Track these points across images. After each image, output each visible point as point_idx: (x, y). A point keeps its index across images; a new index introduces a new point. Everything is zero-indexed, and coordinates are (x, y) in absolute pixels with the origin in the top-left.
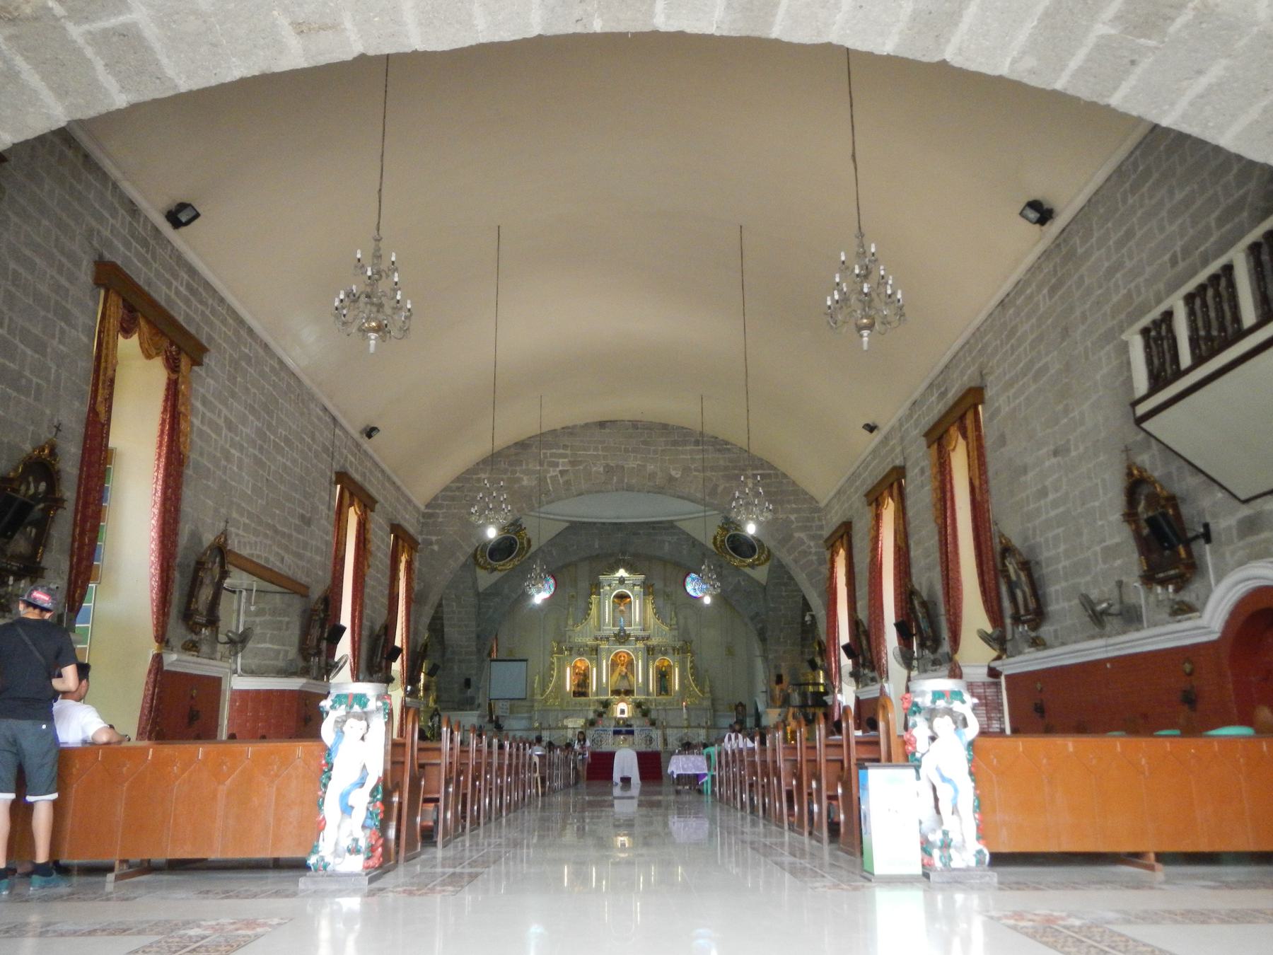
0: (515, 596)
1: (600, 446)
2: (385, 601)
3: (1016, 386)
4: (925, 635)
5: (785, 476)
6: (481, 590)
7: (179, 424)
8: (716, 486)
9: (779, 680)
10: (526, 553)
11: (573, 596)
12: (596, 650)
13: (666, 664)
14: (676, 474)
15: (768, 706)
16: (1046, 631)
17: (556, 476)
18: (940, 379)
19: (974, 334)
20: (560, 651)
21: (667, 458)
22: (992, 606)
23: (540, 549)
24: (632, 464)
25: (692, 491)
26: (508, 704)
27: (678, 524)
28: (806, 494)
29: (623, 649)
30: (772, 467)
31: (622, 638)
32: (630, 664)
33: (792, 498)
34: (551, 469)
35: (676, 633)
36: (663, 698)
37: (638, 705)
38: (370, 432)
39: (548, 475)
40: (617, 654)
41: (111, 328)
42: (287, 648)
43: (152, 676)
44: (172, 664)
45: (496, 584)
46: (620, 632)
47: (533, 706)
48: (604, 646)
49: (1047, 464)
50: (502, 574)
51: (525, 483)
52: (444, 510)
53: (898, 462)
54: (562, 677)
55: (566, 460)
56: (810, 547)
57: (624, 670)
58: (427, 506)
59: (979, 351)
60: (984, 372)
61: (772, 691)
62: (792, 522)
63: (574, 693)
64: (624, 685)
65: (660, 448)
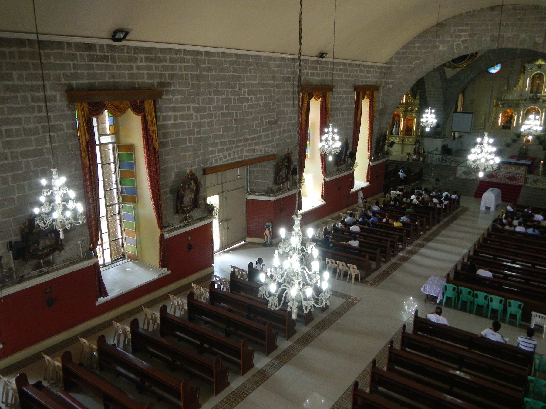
1: (489, 23)
2: (352, 126)
6: (448, 78)
10: (475, 58)
17: (460, 44)
21: (535, 29)
34: (457, 40)
39: (455, 43)
42: (268, 182)
46: (533, 97)
50: (461, 69)
51: (441, 48)
52: (396, 65)
54: (497, 119)
55: (467, 33)
58: (387, 63)
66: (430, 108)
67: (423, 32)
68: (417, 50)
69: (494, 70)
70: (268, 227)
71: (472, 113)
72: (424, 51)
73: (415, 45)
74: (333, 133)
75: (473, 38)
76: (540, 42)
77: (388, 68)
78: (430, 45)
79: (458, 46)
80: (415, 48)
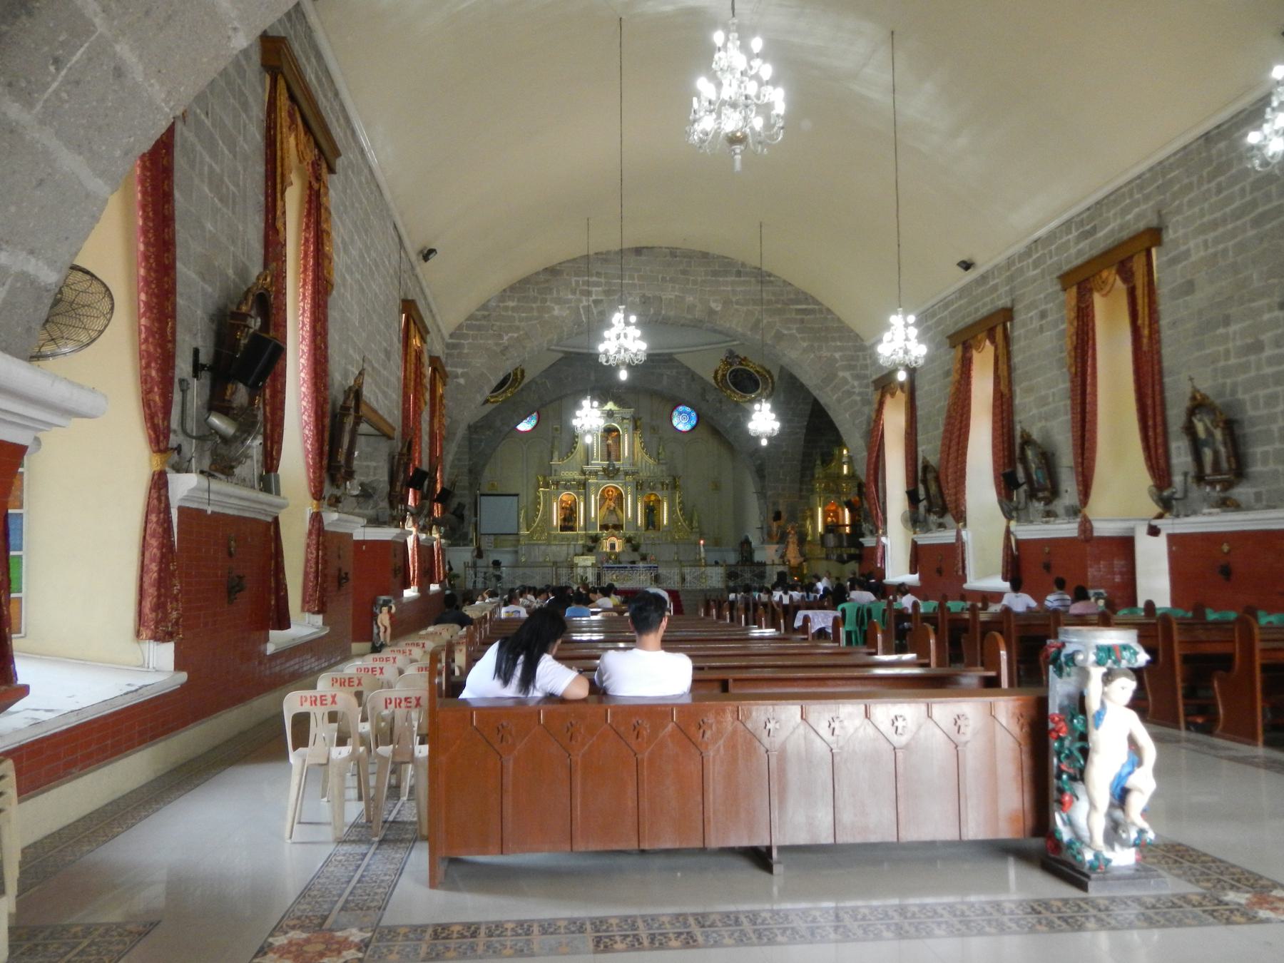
0: (507, 429)
1: (636, 275)
3: (1221, 230)
4: (1036, 486)
5: (829, 311)
7: (323, 244)
8: (758, 321)
9: (777, 516)
11: (556, 429)
12: (583, 485)
13: (653, 498)
14: (717, 307)
15: (763, 543)
16: (1241, 492)
18: (1085, 215)
19: (1151, 169)
20: (547, 485)
22: (1158, 463)
23: (533, 381)
24: (669, 294)
25: (733, 326)
26: (492, 538)
27: (676, 356)
28: (852, 331)
29: (611, 484)
30: (816, 302)
31: (610, 473)
32: (620, 498)
33: (836, 335)
35: (664, 468)
36: (652, 534)
37: (629, 540)
38: (427, 254)
39: (581, 305)
40: (603, 491)
41: (284, 124)
43: (314, 537)
44: (333, 523)
45: (486, 416)
47: (519, 541)
48: (592, 480)
49: (1266, 317)
50: (495, 405)
51: (556, 312)
53: (1004, 302)
54: (548, 512)
56: (853, 387)
57: (613, 505)
58: (451, 336)
59: (1158, 187)
60: (1164, 212)
61: (770, 527)
62: (836, 361)
63: (563, 528)
64: (612, 520)
65: (699, 279)
66: (589, 397)
67: (520, 282)
68: (510, 313)
69: (524, 426)
70: (386, 603)
71: (517, 495)
72: (524, 315)
73: (507, 304)
74: (627, 323)
75: (611, 298)
76: (719, 309)
77: (454, 346)
78: (534, 305)
79: (588, 309)
80: (506, 308)
